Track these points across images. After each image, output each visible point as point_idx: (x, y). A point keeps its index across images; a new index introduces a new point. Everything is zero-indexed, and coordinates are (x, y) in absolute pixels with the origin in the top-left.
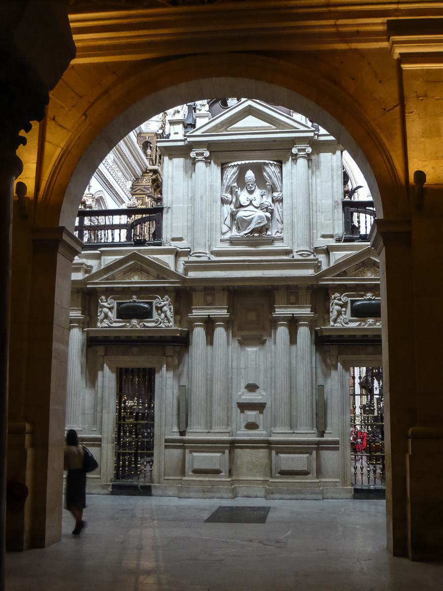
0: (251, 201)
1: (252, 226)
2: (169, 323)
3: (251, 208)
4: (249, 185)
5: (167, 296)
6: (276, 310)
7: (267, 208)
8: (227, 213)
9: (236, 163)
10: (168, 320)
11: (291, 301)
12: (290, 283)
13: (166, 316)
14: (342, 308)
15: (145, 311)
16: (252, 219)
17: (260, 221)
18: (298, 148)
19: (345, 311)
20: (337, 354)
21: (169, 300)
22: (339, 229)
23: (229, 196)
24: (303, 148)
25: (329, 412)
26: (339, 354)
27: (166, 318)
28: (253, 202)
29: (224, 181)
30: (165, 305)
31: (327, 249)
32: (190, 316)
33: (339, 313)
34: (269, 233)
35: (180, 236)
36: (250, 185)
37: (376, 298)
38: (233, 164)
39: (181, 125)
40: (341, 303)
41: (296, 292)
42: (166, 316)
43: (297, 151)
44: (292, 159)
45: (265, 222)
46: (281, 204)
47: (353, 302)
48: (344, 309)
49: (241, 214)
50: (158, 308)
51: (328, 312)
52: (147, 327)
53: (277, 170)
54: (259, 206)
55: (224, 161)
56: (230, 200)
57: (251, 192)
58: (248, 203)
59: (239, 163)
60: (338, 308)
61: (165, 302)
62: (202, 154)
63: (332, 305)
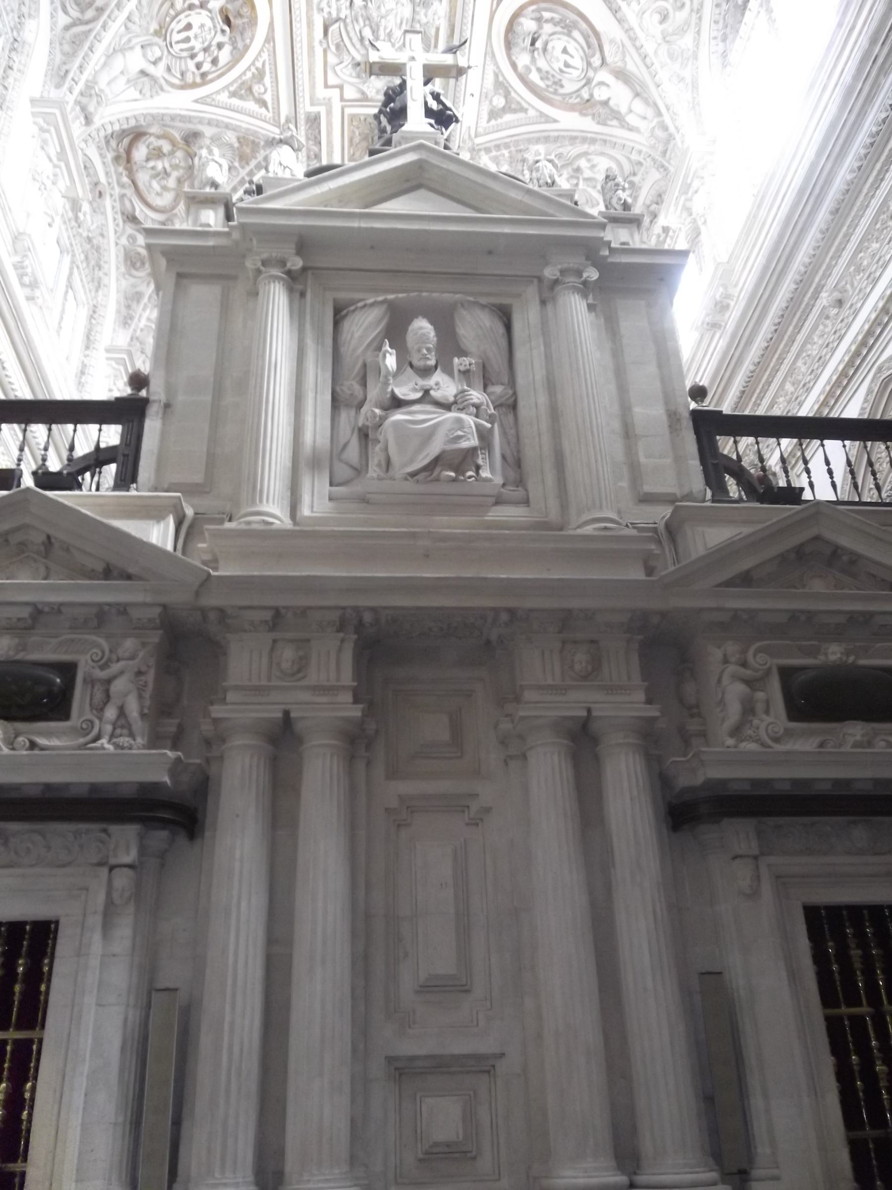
0: (427, 392)
1: (435, 448)
2: (132, 735)
3: (429, 408)
4: (419, 351)
5: (129, 644)
6: (528, 695)
7: (477, 407)
8: (348, 431)
9: (380, 298)
10: (128, 726)
11: (577, 667)
12: (575, 604)
13: (122, 712)
14: (754, 689)
15: (42, 689)
16: (436, 427)
17: (460, 433)
18: (559, 267)
19: (768, 703)
20: (756, 852)
21: (141, 654)
22: (696, 480)
23: (357, 388)
24: (576, 266)
25: (754, 1083)
26: (762, 854)
27: (122, 721)
28: (432, 392)
29: (343, 350)
30: (122, 673)
31: (668, 526)
32: (217, 711)
33: (749, 709)
34: (485, 474)
35: (199, 478)
36: (425, 351)
37: (863, 662)
38: (371, 301)
39: (221, 211)
40: (748, 673)
41: (592, 642)
42: (122, 712)
43: (558, 274)
44: (543, 303)
45: (474, 442)
46: (511, 417)
47: (786, 674)
48: (760, 695)
49: (398, 416)
50: (90, 682)
51: (694, 710)
52: (42, 749)
53: (501, 329)
54: (452, 399)
55: (343, 296)
56: (361, 396)
57: (426, 372)
58: (418, 395)
59: (391, 297)
60: (741, 688)
61: (121, 664)
62: (282, 263)
63: (719, 681)
